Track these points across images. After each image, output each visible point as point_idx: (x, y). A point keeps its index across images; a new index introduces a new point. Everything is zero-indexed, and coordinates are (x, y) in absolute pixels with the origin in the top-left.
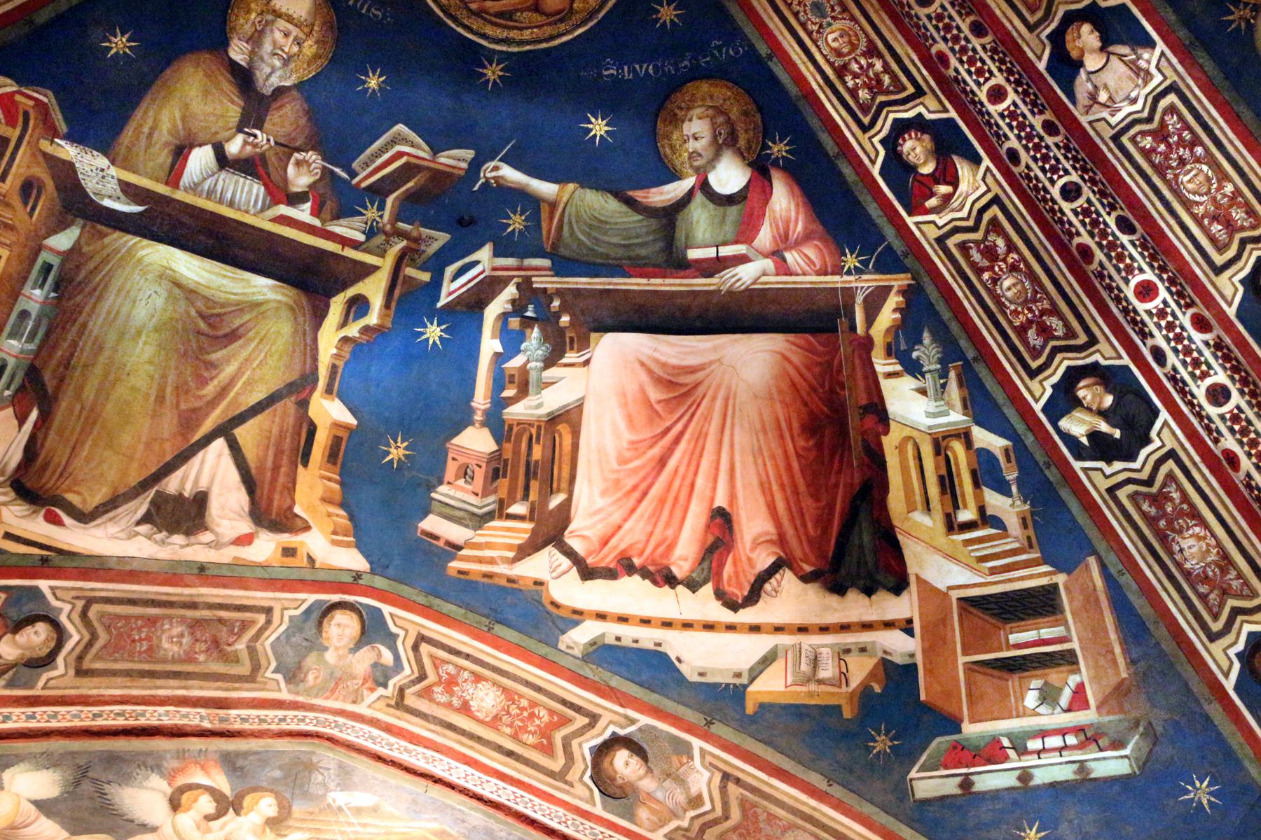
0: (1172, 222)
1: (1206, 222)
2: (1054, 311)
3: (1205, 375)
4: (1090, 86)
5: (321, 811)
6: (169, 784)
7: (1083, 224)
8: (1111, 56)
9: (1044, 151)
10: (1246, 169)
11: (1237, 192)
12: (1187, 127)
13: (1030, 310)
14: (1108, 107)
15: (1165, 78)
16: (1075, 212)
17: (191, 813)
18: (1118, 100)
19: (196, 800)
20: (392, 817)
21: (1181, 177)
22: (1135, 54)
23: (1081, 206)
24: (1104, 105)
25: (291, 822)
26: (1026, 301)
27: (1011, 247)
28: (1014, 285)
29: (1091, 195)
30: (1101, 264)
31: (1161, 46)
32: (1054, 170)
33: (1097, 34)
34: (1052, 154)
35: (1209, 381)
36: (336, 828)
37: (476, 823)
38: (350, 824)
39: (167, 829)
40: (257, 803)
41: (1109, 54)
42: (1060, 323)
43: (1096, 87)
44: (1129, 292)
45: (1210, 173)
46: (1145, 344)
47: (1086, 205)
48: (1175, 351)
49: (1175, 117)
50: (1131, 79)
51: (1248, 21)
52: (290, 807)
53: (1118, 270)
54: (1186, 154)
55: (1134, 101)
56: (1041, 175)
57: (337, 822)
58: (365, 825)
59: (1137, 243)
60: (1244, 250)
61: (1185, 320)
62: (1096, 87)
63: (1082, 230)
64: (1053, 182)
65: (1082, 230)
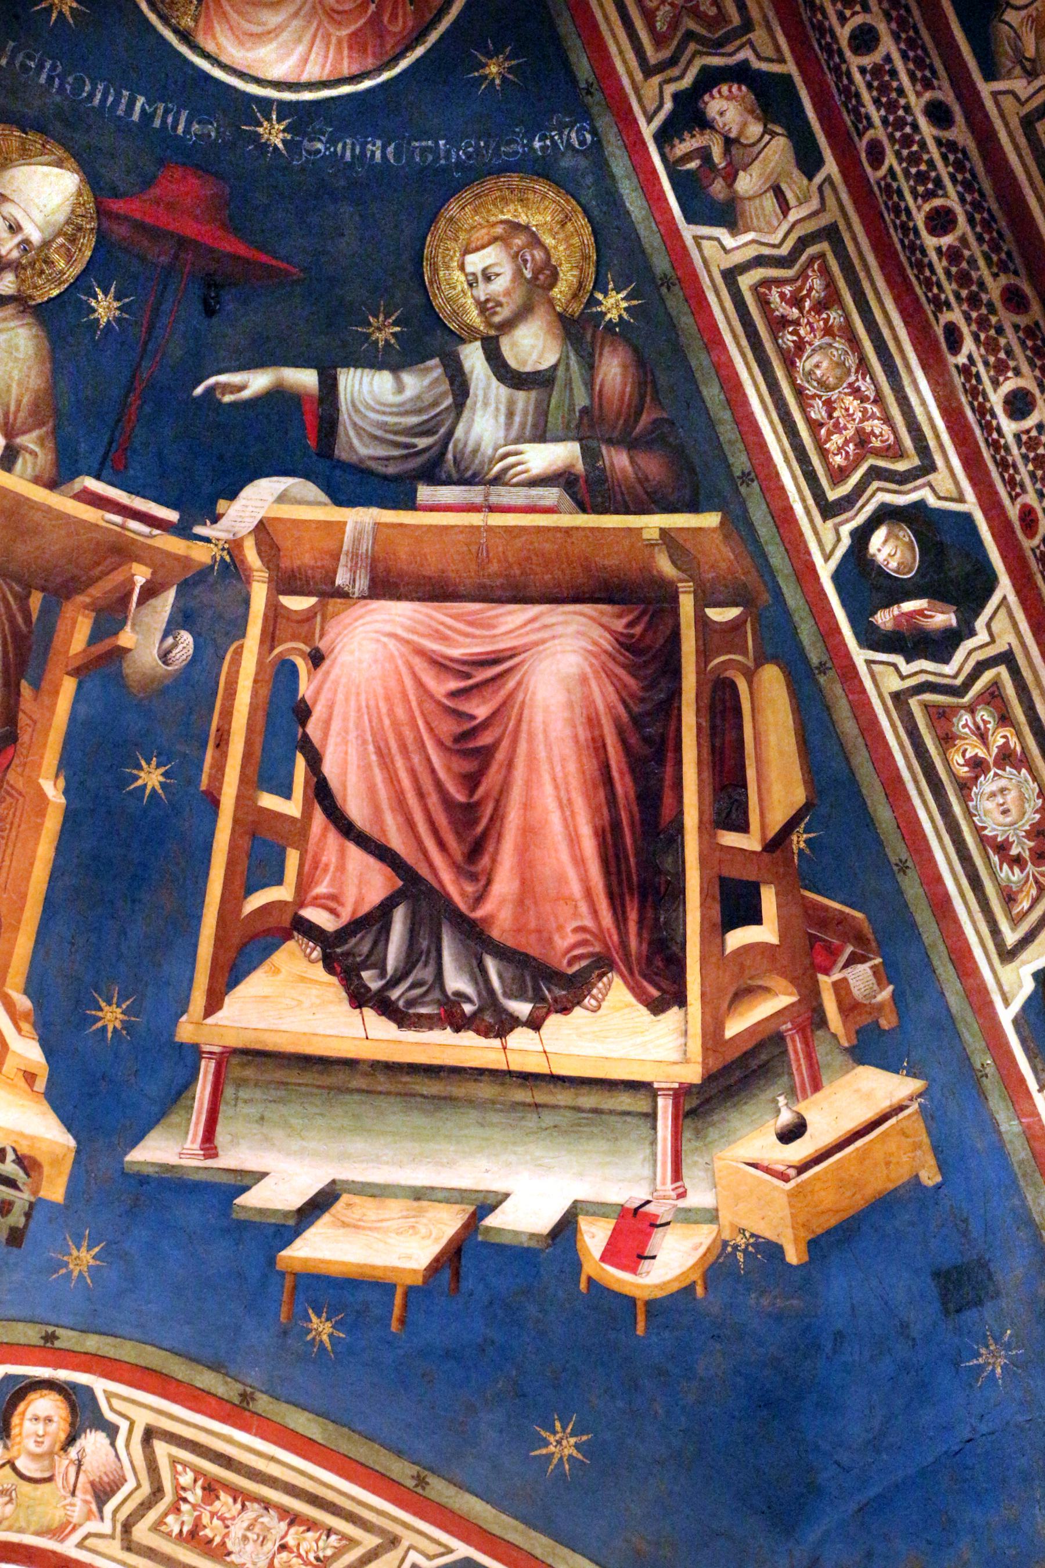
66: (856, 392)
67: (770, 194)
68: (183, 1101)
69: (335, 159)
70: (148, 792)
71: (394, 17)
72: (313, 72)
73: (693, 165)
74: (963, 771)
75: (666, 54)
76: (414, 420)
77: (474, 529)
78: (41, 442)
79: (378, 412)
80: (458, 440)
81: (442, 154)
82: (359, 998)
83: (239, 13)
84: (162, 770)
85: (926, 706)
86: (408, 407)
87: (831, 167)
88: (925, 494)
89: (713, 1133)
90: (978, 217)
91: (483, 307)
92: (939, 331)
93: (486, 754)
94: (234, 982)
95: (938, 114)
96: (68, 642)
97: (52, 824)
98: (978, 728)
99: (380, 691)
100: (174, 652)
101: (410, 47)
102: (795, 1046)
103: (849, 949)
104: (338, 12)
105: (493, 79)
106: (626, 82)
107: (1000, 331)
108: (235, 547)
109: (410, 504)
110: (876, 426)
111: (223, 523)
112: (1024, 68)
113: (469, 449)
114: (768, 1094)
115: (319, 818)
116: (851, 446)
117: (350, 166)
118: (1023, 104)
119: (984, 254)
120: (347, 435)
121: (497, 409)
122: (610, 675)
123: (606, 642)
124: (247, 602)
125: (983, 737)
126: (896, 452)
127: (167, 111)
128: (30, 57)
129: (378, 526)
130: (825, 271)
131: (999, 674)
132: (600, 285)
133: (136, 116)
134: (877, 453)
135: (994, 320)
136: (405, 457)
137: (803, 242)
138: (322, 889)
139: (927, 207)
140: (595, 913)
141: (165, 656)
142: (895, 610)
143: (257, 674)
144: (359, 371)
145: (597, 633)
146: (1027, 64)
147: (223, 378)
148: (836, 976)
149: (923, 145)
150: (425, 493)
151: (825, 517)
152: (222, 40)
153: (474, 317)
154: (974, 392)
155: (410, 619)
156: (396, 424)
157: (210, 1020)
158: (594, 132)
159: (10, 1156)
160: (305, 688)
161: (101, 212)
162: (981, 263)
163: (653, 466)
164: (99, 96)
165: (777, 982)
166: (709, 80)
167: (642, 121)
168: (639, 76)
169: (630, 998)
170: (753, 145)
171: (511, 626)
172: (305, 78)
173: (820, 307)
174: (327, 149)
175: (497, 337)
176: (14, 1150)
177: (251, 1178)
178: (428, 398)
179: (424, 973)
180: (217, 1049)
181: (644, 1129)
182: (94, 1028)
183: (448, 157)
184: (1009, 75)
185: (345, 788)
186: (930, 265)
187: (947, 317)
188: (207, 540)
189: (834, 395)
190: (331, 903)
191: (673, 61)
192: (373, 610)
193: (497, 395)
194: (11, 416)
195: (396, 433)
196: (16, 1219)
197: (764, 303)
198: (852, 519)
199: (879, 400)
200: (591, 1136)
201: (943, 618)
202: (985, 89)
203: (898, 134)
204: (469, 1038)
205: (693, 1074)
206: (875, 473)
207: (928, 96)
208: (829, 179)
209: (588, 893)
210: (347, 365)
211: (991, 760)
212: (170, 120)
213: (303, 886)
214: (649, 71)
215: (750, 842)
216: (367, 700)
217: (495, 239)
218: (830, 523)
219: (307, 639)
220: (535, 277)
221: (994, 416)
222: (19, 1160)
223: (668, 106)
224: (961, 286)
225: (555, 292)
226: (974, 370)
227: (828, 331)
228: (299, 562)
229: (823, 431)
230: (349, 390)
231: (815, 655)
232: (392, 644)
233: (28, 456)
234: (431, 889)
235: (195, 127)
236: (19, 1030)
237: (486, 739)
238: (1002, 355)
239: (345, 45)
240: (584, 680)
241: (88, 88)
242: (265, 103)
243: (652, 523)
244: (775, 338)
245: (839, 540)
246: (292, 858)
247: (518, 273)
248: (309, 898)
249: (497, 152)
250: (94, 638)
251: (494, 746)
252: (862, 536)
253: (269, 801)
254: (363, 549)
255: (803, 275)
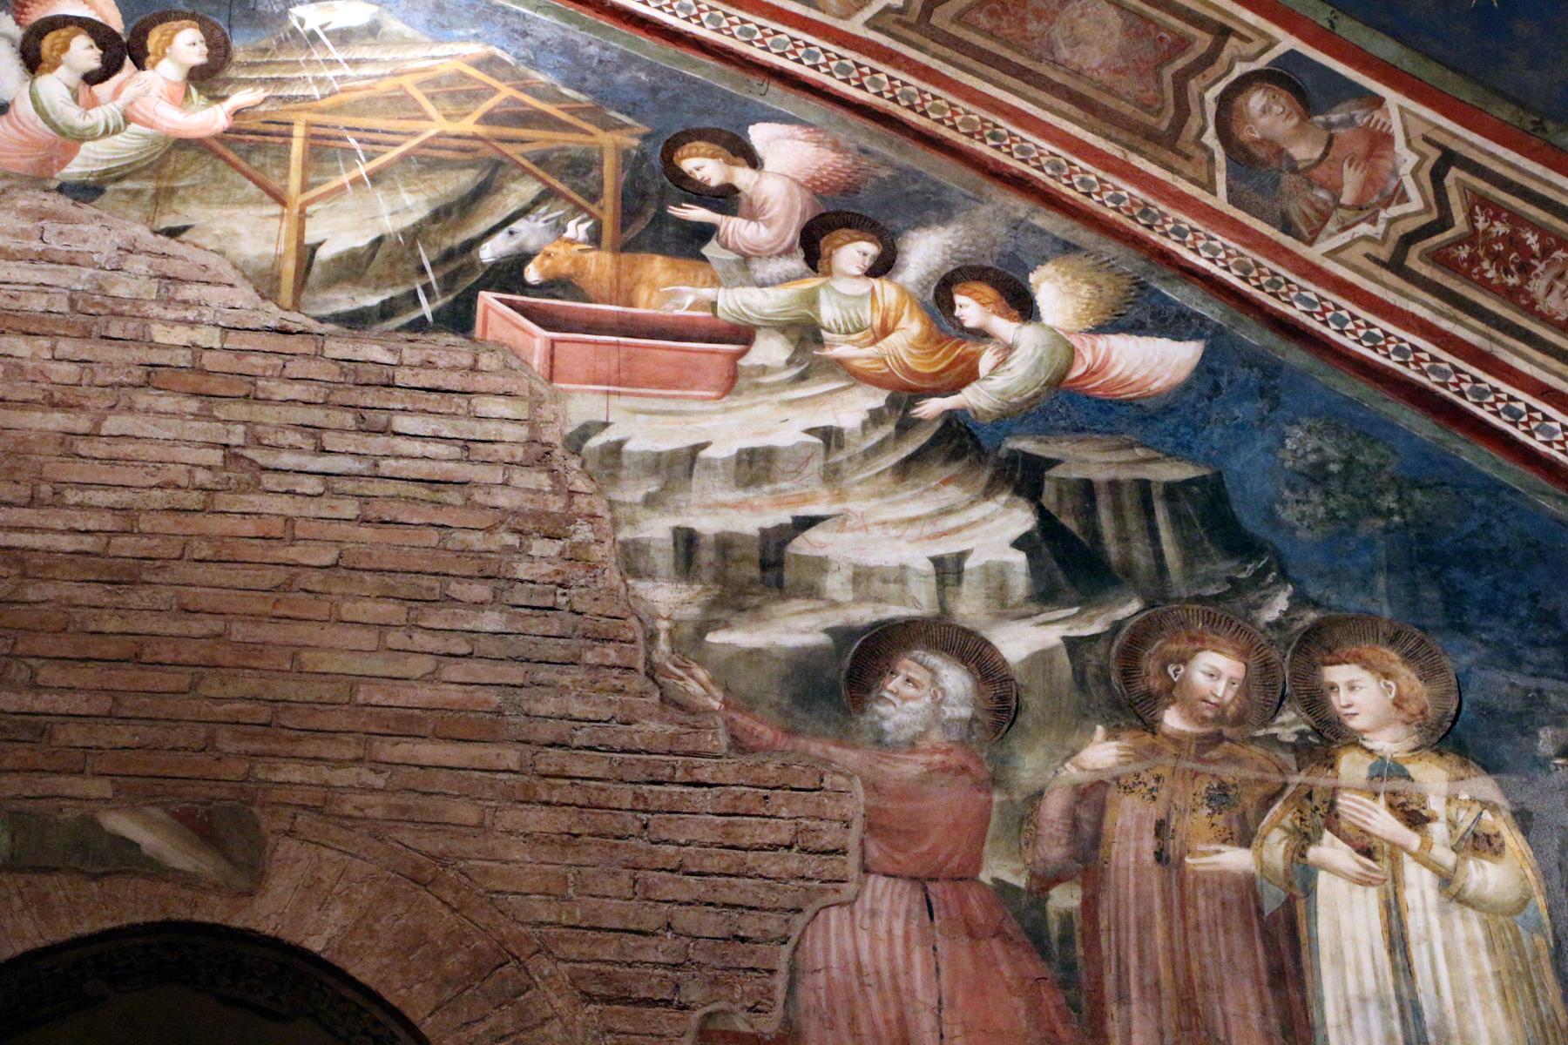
5: (280, 42)
6: (18, 22)
17: (62, 71)
19: (66, 48)
20: (405, 42)
25: (232, 73)
36: (308, 73)
37: (545, 34)
38: (332, 63)
39: (24, 108)
40: (170, 42)
52: (227, 43)
57: (309, 62)
58: (355, 63)
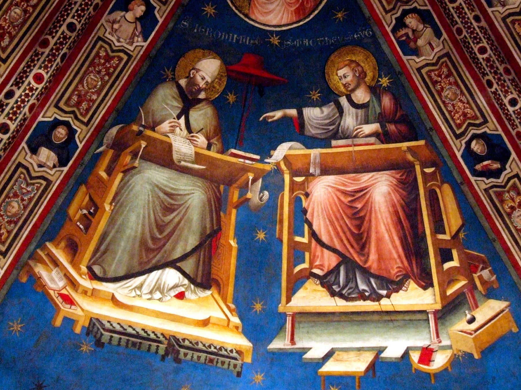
0: (71, 78)
1: (76, 93)
2: (12, 38)
3: (11, 119)
4: (119, 18)
7: (59, 38)
8: (134, 24)
9: (86, 8)
10: (105, 102)
11: (94, 101)
12: (115, 68)
13: (9, 26)
14: (112, 30)
15: (133, 52)
16: (63, 33)
18: (117, 33)
21: (92, 74)
22: (139, 35)
23: (67, 34)
24: (112, 28)
26: (12, 23)
27: (34, 7)
28: (18, 15)
29: (73, 37)
30: (43, 53)
31: (146, 44)
32: (79, 16)
33: (142, 14)
34: (85, 12)
35: (9, 122)
41: (135, 22)
42: (7, 43)
43: (119, 21)
44: (35, 71)
45: (98, 86)
46: (12, 86)
47: (68, 36)
48: (17, 102)
49: (118, 62)
50: (127, 36)
51: (167, 78)
53: (43, 62)
54: (103, 73)
55: (119, 41)
56: (74, 11)
59: (58, 66)
60: (70, 114)
61: (32, 101)
62: (119, 21)
63: (56, 38)
64: (73, 17)
65: (56, 38)
66: (461, 101)
67: (428, 45)
68: (283, 330)
69: (294, 46)
70: (261, 240)
71: (307, 3)
72: (284, 22)
73: (404, 38)
74: (508, 210)
75: (391, 6)
76: (327, 121)
77: (350, 152)
78: (217, 140)
79: (315, 119)
80: (342, 126)
81: (327, 42)
82: (333, 294)
83: (261, 6)
84: (264, 233)
85: (495, 192)
86: (325, 118)
87: (445, 35)
88: (486, 129)
89: (447, 323)
90: (493, 48)
91: (345, 86)
92: (484, 82)
93: (362, 219)
94: (294, 293)
95: (477, 19)
96: (232, 198)
97: (234, 253)
98: (511, 197)
99: (327, 202)
100: (263, 197)
101: (313, 11)
102: (469, 296)
103: (481, 266)
104: (291, 3)
105: (340, 19)
106: (380, 16)
107: (505, 81)
108: (278, 164)
109: (330, 147)
110: (469, 110)
111: (273, 157)
112: (501, 4)
113: (346, 128)
114: (462, 311)
115: (314, 242)
116: (462, 117)
117: (299, 47)
118: (502, 14)
119: (497, 59)
120: (308, 127)
121: (353, 115)
122: (397, 191)
123: (395, 182)
124: (283, 180)
125: (513, 200)
126: (475, 118)
127: (243, 38)
128: (203, 28)
129: (321, 154)
130: (447, 66)
131: (515, 181)
132: (380, 76)
133: (234, 41)
134: (469, 118)
135: (502, 78)
136: (326, 133)
137: (439, 58)
138: (317, 263)
139: (478, 46)
140: (402, 262)
141: (261, 199)
142: (481, 164)
143: (289, 201)
144: (309, 108)
145: (391, 179)
146: (502, 3)
147: (268, 114)
148: (478, 274)
149: (474, 28)
150: (334, 143)
151: (457, 139)
152: (256, 14)
153: (342, 89)
154: (498, 99)
155: (334, 180)
156: (322, 123)
157: (288, 305)
158: (372, 31)
159: (234, 351)
160: (305, 204)
161: (228, 70)
162: (496, 61)
163: (402, 128)
164: (223, 36)
165: (461, 277)
166: (405, 13)
167: (386, 27)
168: (384, 14)
169: (416, 286)
170: (421, 31)
171: (365, 180)
172: (282, 23)
173: (447, 77)
174: (292, 43)
175: (350, 95)
176: (235, 349)
177: (306, 350)
178: (331, 115)
179: (351, 285)
180: (291, 313)
181: (426, 324)
182: (253, 311)
183: (329, 41)
184: (496, 6)
185: (320, 232)
186: (481, 63)
187: (487, 78)
188: (269, 163)
189: (455, 102)
190: (321, 267)
191: (394, 9)
192: (323, 179)
193: (352, 111)
194: (208, 134)
195: (323, 126)
196: (238, 369)
197: (430, 77)
198: (465, 138)
199: (468, 103)
200: (409, 328)
201: (496, 166)
202: (489, 10)
203: (466, 26)
204: (368, 303)
205: (439, 307)
206: (470, 125)
207: (473, 14)
208: (445, 39)
209: (399, 256)
210: (305, 107)
211: (516, 206)
212: (244, 40)
213: (311, 263)
214: (387, 12)
215: (447, 237)
216: (324, 206)
217: (346, 65)
218: (458, 140)
219: (304, 189)
220: (360, 75)
221: (505, 106)
222: (237, 352)
223: (394, 22)
224: (491, 69)
225: (366, 79)
226: (498, 93)
227: (450, 84)
228: (298, 167)
229: (452, 113)
230: (307, 114)
231: (459, 180)
232: (330, 189)
233: (215, 146)
234: (350, 259)
235: (252, 42)
236: (232, 315)
237: (362, 214)
238: (506, 88)
239: (294, 13)
240: (389, 193)
241: (220, 34)
242: (271, 32)
243: (405, 145)
244: (434, 87)
245: (462, 145)
246: (307, 255)
247: (354, 75)
248: (313, 266)
249: (343, 40)
250: (240, 196)
251: (365, 215)
252: (468, 143)
253: (298, 239)
254: (317, 161)
255: (441, 68)
